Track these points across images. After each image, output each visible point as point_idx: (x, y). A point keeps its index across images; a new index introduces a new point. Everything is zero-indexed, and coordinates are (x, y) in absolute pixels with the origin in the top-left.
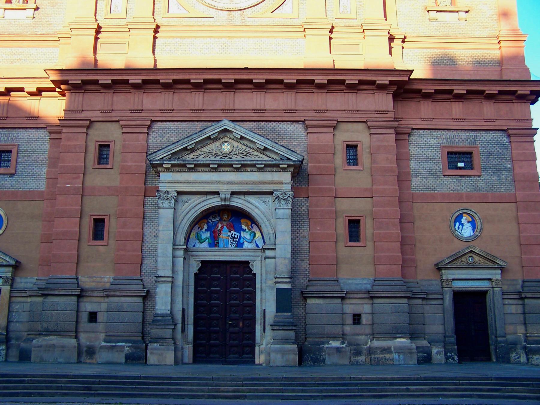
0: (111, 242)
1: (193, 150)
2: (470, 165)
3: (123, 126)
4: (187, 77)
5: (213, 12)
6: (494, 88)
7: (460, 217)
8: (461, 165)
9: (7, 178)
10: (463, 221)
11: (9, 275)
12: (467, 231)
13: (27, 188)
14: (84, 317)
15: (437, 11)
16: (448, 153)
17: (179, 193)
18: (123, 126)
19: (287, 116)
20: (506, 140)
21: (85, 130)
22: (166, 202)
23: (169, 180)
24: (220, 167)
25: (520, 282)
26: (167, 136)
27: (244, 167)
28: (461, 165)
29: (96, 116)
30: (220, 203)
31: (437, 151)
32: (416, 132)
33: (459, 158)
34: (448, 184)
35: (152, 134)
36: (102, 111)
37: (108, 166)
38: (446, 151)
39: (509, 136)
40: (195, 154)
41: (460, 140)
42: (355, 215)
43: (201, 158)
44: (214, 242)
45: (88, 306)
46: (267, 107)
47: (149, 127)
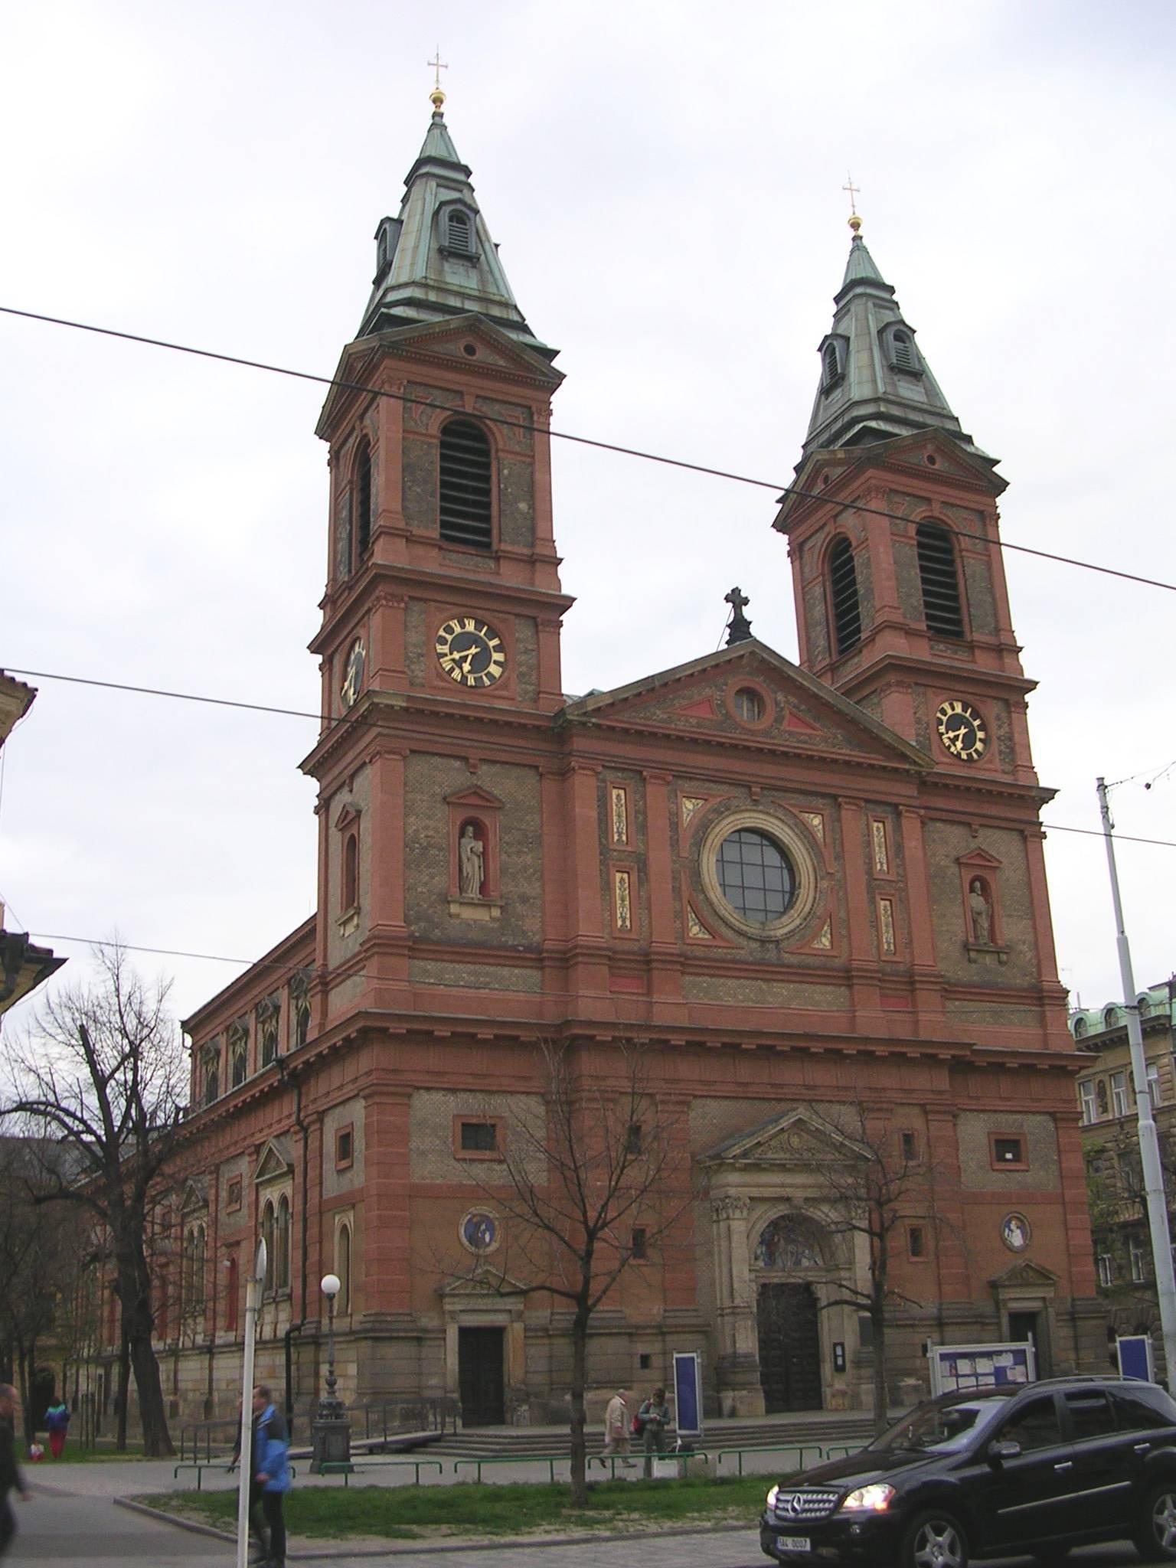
2: (1017, 1158)
4: (738, 1041)
5: (744, 942)
7: (1009, 1221)
8: (1009, 1156)
10: (1013, 1226)
12: (1017, 1239)
16: (997, 1141)
17: (751, 1199)
20: (1051, 1125)
22: (738, 1212)
23: (733, 1183)
25: (1069, 1299)
26: (707, 1117)
28: (1009, 1156)
31: (983, 1139)
32: (963, 1115)
33: (1007, 1146)
34: (996, 1182)
38: (994, 1137)
39: (1055, 1120)
41: (1008, 1123)
44: (771, 1258)
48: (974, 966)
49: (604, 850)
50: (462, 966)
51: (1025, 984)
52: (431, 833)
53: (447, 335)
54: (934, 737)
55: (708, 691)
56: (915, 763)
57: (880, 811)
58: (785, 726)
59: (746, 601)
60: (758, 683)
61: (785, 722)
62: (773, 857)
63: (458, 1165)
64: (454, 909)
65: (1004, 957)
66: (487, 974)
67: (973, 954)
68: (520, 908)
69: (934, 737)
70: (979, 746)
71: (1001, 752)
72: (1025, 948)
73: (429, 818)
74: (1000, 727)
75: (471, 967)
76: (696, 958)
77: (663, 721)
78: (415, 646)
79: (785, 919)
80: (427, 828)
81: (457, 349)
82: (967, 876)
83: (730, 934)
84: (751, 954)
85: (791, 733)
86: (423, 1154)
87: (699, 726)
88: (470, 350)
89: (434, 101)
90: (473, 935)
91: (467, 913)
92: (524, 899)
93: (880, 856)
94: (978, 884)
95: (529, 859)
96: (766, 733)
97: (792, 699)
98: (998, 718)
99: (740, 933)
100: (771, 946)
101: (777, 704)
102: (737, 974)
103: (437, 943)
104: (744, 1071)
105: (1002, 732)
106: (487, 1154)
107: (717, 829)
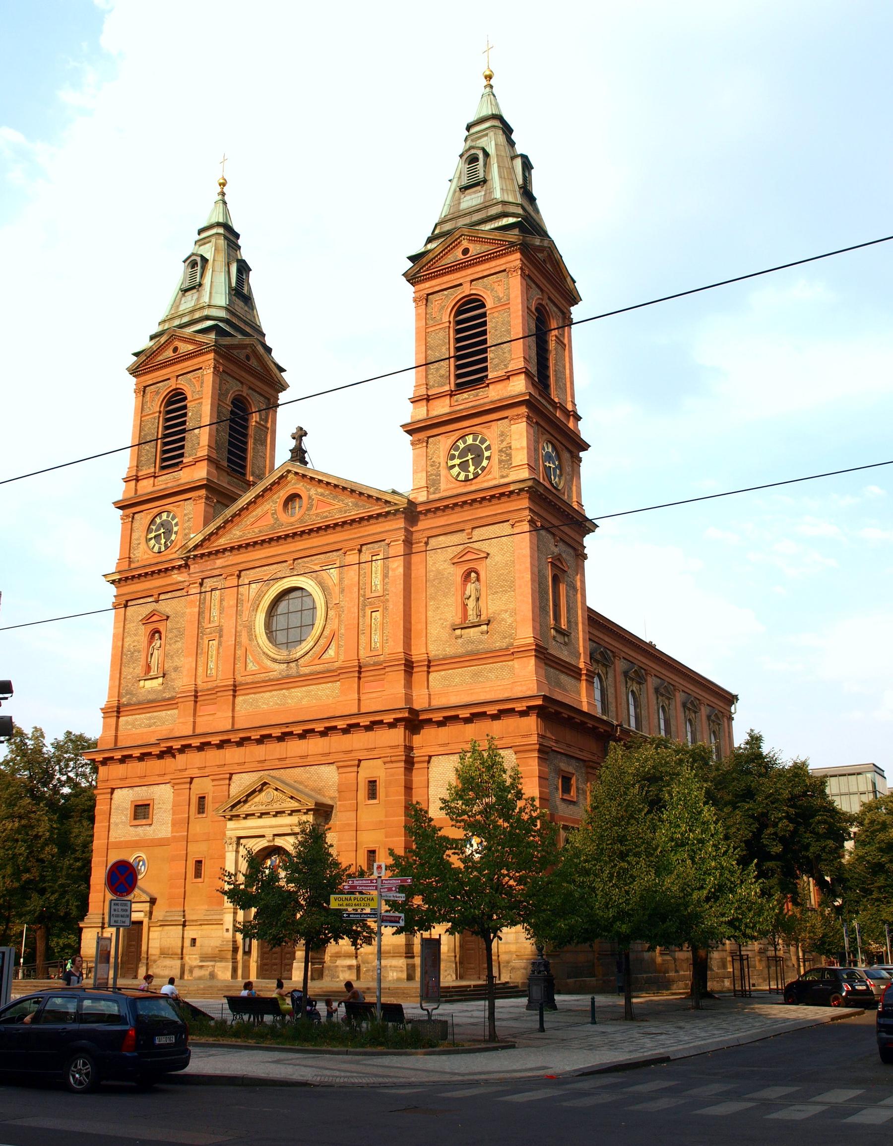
0: (206, 880)
1: (246, 802)
3: (213, 780)
4: (249, 735)
5: (276, 666)
6: (493, 708)
9: (147, 828)
11: (148, 909)
13: (160, 836)
14: (187, 943)
15: (462, 628)
18: (213, 780)
19: (324, 760)
21: (188, 786)
24: (262, 815)
27: (278, 813)
29: (195, 772)
30: (267, 844)
35: (233, 785)
36: (199, 768)
37: (204, 815)
40: (249, 804)
42: (372, 846)
43: (253, 808)
45: (190, 933)
46: (310, 753)
47: (230, 779)
48: (460, 641)
49: (200, 631)
50: (143, 715)
51: (504, 645)
52: (136, 644)
53: (161, 348)
54: (443, 472)
55: (268, 507)
56: (396, 504)
57: (376, 545)
58: (313, 511)
59: (306, 434)
60: (299, 487)
61: (314, 508)
62: (282, 607)
63: (132, 829)
64: (142, 683)
65: (484, 628)
66: (154, 718)
67: (458, 632)
68: (174, 675)
69: (443, 472)
70: (485, 463)
71: (500, 462)
72: (505, 616)
73: (136, 635)
74: (502, 441)
75: (148, 715)
76: (247, 684)
77: (241, 537)
78: (137, 540)
79: (304, 644)
80: (134, 641)
81: (169, 353)
82: (460, 571)
83: (269, 663)
84: (280, 674)
85: (317, 515)
86: (117, 825)
87: (260, 532)
88: (175, 349)
89: (486, 77)
90: (150, 697)
91: (149, 684)
92: (176, 669)
93: (377, 580)
94: (473, 575)
95: (179, 645)
96: (301, 520)
97: (320, 490)
98: (502, 434)
99: (274, 660)
100: (293, 665)
101: (310, 497)
102: (270, 688)
103: (135, 704)
104: (260, 751)
105: (505, 444)
106: (144, 822)
107: (266, 597)
